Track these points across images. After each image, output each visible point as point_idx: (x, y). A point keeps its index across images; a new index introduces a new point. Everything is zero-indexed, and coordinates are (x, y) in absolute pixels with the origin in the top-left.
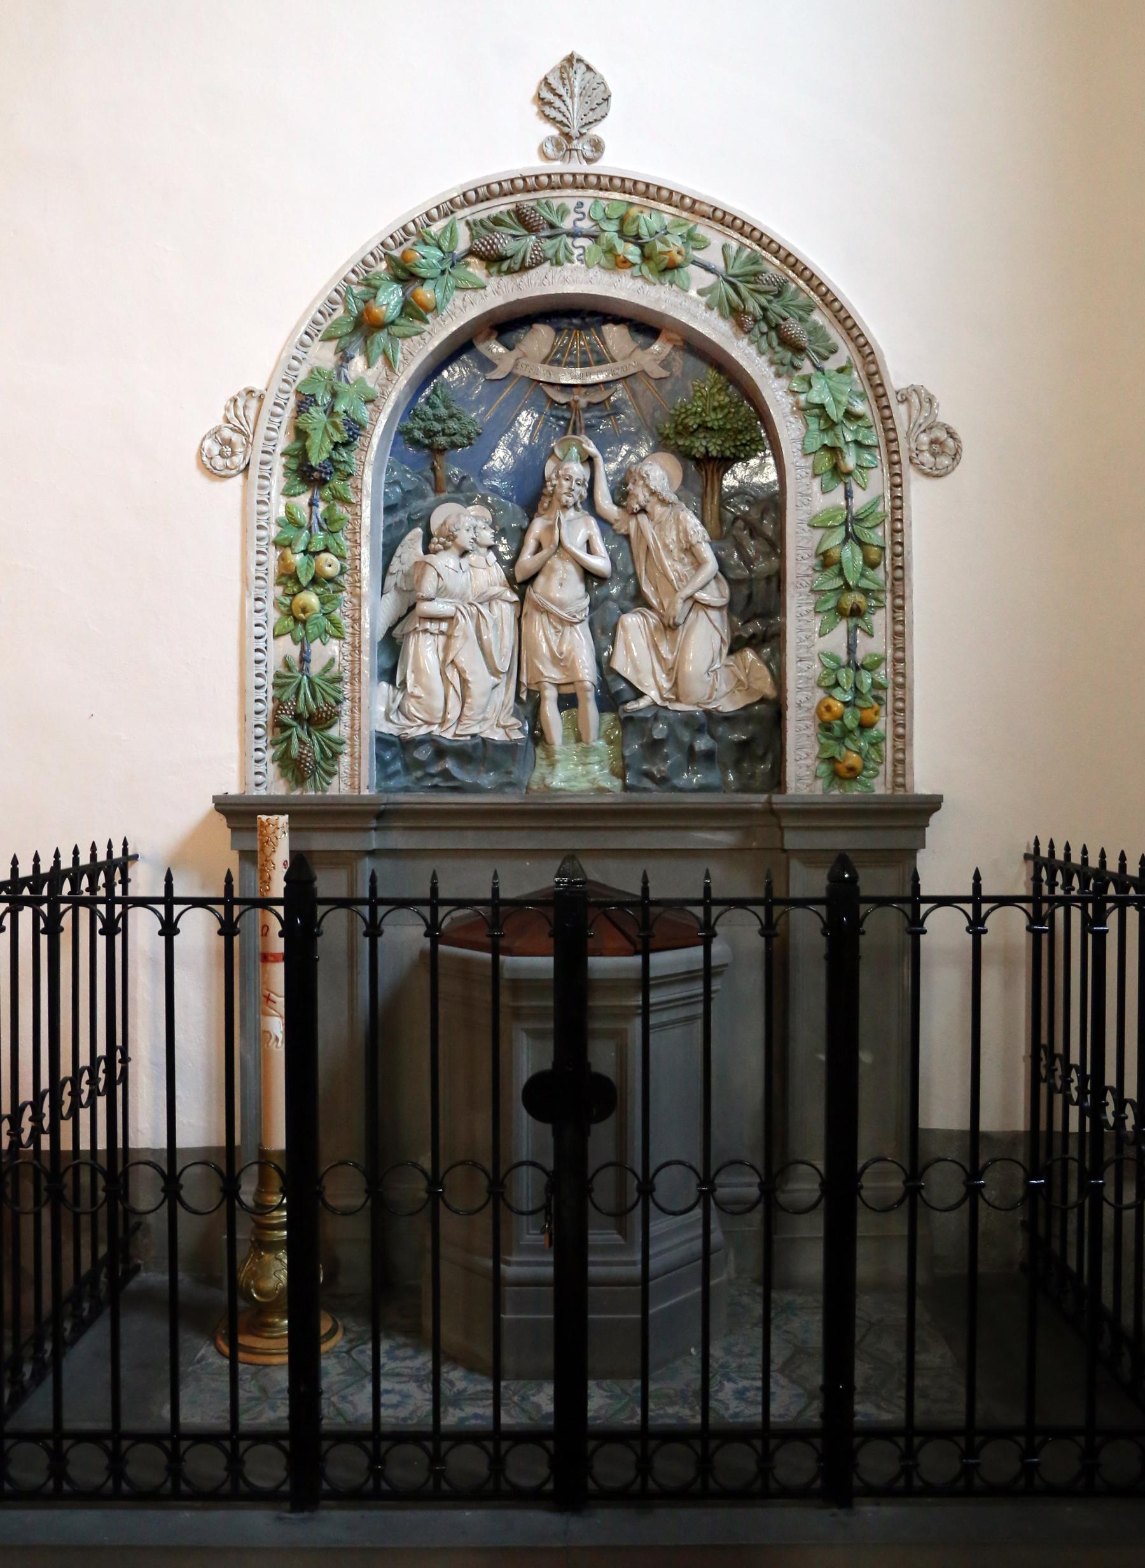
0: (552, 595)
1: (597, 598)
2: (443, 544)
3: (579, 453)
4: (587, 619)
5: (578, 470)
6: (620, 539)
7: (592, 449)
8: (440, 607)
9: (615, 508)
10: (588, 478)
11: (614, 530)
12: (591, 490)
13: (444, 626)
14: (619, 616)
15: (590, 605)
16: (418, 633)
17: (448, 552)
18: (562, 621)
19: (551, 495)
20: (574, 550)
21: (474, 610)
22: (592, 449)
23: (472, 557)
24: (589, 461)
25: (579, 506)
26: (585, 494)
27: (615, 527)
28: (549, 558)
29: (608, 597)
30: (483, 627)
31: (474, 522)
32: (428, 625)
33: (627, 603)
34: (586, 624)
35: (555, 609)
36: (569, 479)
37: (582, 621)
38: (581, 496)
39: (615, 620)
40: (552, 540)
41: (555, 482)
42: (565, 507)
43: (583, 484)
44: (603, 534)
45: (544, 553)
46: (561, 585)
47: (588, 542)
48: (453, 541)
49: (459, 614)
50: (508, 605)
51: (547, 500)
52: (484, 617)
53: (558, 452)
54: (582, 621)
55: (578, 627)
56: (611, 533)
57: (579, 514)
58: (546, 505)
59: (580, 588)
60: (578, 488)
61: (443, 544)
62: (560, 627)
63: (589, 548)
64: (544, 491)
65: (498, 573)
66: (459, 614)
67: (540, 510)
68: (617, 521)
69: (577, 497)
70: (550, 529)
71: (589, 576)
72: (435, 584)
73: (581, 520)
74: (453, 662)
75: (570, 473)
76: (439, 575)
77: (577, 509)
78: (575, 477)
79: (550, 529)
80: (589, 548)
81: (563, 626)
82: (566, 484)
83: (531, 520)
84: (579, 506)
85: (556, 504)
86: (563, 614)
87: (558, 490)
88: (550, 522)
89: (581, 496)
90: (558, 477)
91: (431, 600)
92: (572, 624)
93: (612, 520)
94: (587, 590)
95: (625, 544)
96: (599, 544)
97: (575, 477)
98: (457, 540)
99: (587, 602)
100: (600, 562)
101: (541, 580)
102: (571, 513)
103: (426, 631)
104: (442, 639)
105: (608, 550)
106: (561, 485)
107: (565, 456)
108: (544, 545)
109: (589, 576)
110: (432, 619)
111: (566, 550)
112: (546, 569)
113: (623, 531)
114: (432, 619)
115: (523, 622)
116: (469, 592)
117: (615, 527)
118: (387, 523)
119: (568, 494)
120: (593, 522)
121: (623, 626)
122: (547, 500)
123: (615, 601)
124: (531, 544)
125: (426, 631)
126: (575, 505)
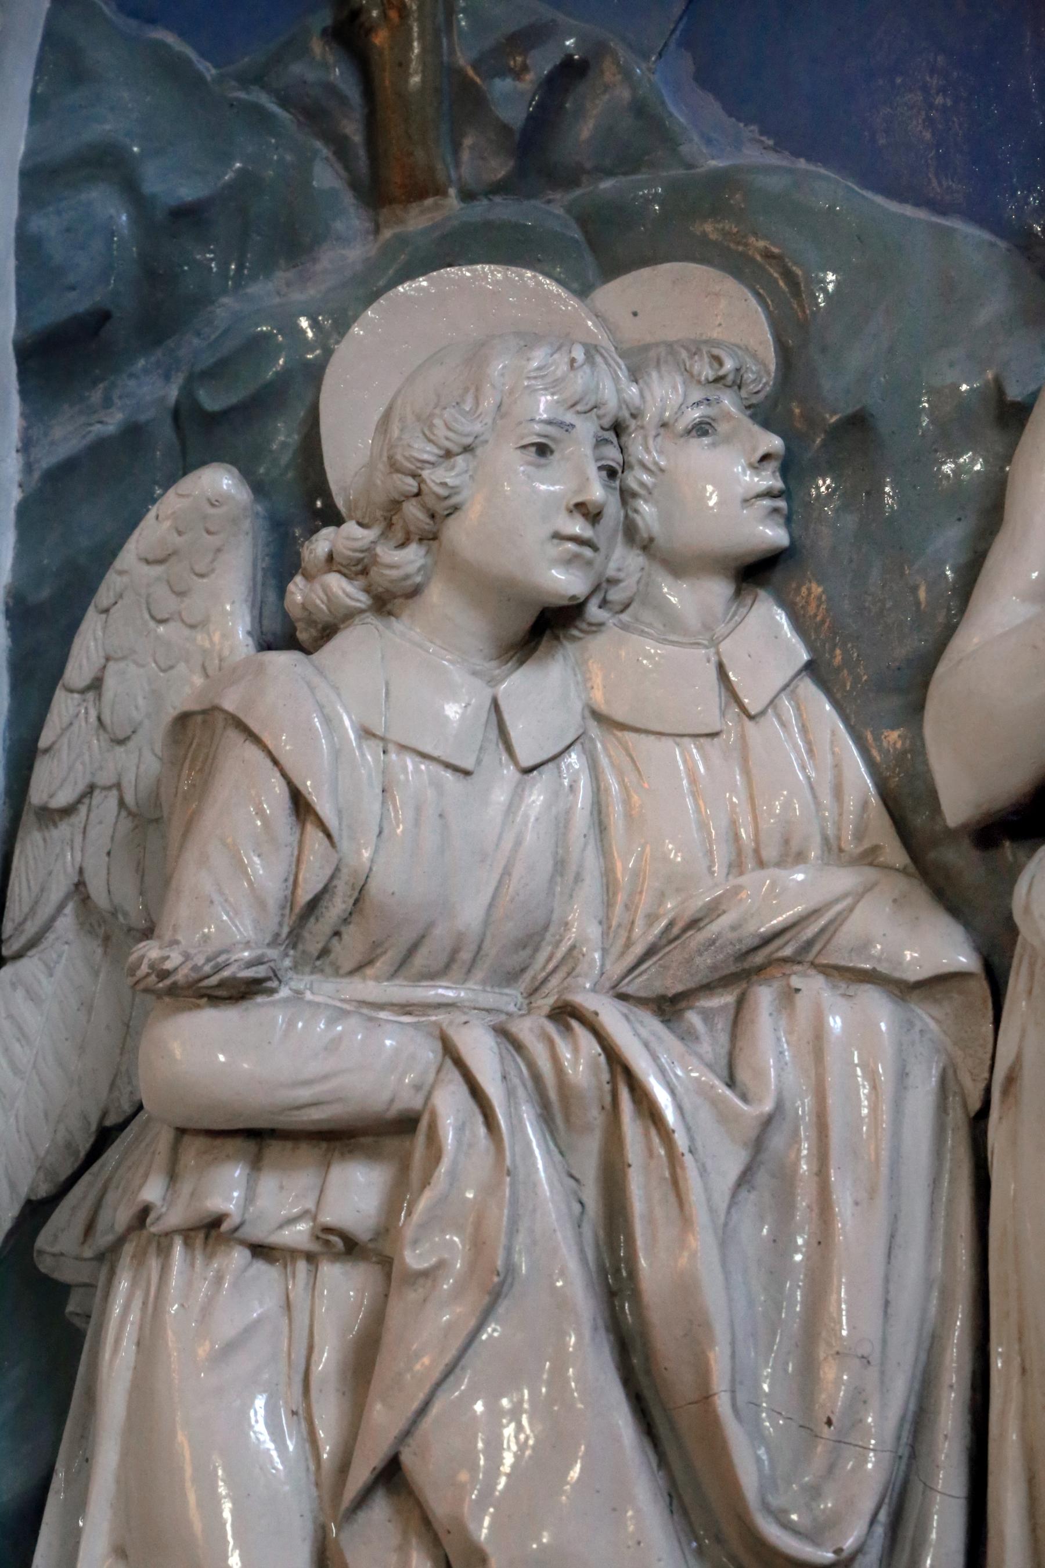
2: (359, 568)
8: (314, 1045)
13: (356, 1192)
16: (162, 1245)
17: (404, 631)
21: (579, 1060)
23: (609, 664)
30: (641, 1191)
31: (613, 389)
32: (225, 1187)
48: (430, 538)
49: (451, 1107)
50: (881, 1014)
52: (651, 1113)
61: (359, 568)
65: (814, 763)
66: (451, 1107)
72: (265, 872)
74: (391, 1475)
76: (300, 806)
91: (242, 991)
98: (460, 533)
103: (211, 1231)
104: (342, 1287)
110: (259, 1138)
114: (259, 1138)
116: (582, 923)
118: (47, 460)
125: (211, 1231)
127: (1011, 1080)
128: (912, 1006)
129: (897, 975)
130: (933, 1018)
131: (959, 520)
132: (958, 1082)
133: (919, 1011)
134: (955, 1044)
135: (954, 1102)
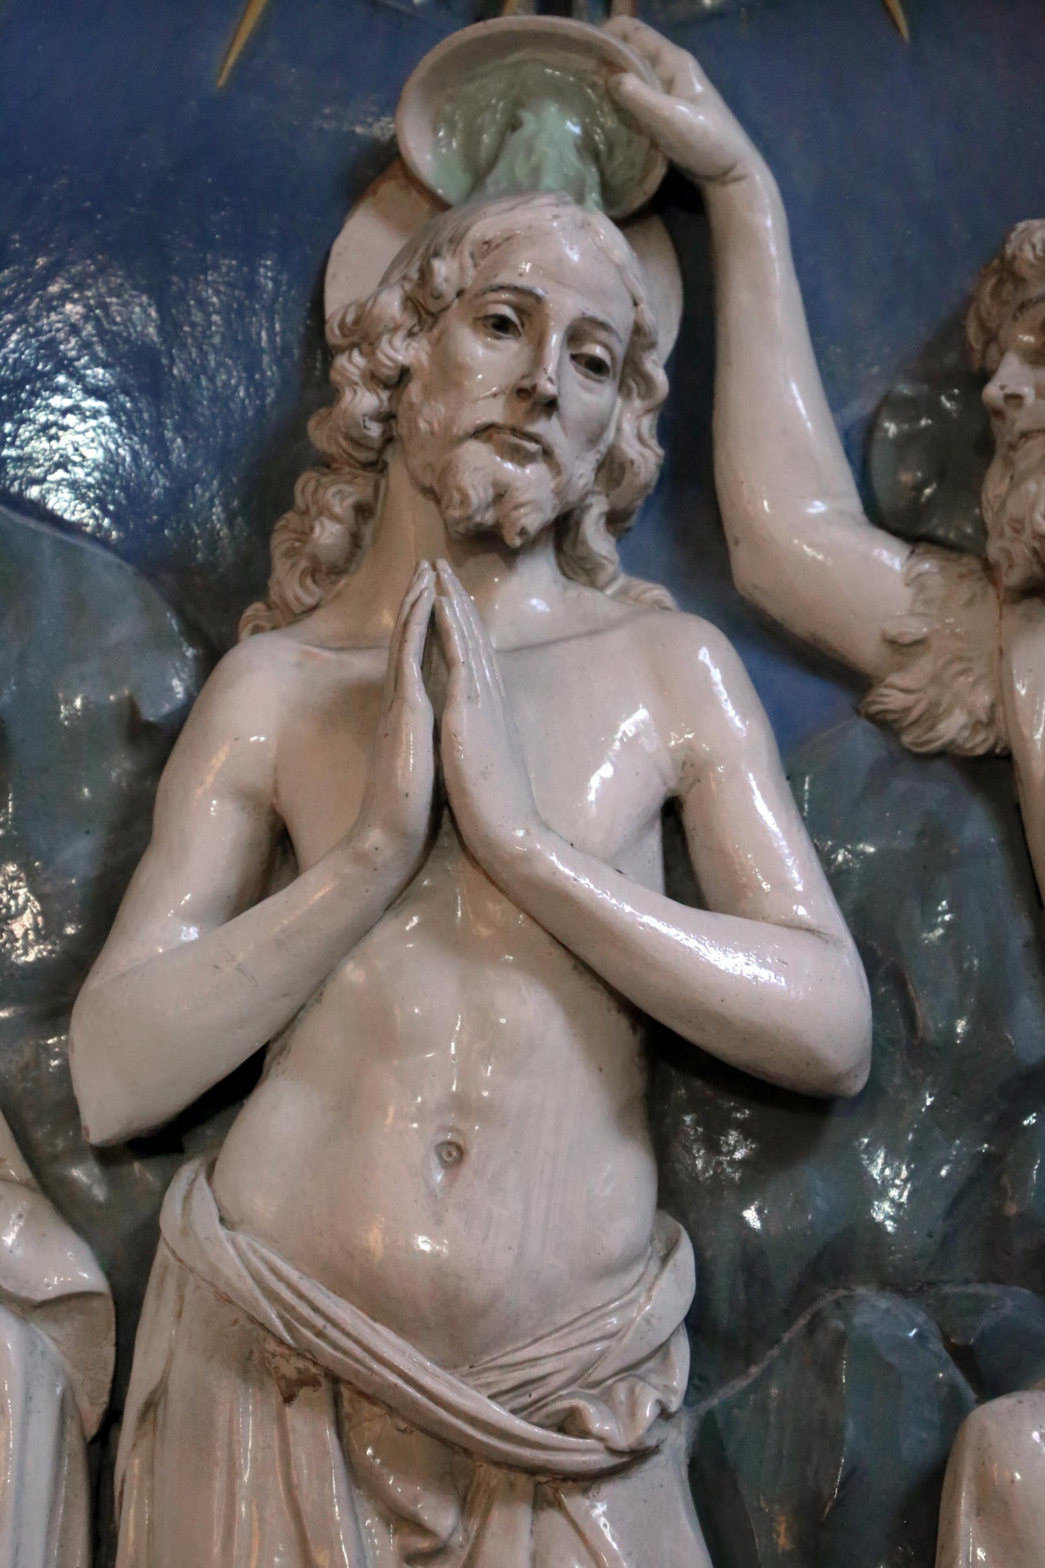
0: (374, 1239)
1: (752, 1255)
3: (587, 148)
4: (677, 1440)
5: (581, 257)
6: (937, 791)
7: (694, 111)
9: (890, 556)
10: (667, 338)
11: (886, 725)
12: (691, 419)
14: (953, 1414)
15: (698, 1322)
18: (462, 1464)
19: (377, 466)
20: (560, 865)
22: (694, 111)
24: (675, 209)
25: (598, 540)
26: (645, 457)
27: (890, 699)
28: (355, 937)
29: (844, 1255)
33: (1011, 1303)
34: (666, 1479)
35: (401, 1357)
36: (516, 318)
37: (635, 1458)
38: (612, 468)
39: (916, 1443)
40: (375, 795)
41: (400, 351)
42: (486, 544)
43: (628, 374)
44: (797, 752)
45: (313, 893)
46: (453, 1154)
47: (671, 812)
51: (339, 497)
53: (427, 149)
54: (635, 1458)
55: (598, 1511)
56: (861, 743)
57: (599, 603)
58: (328, 534)
59: (620, 1179)
60: (584, 398)
62: (442, 1517)
63: (682, 853)
64: (320, 435)
67: (288, 583)
68: (902, 649)
69: (582, 470)
70: (366, 710)
71: (680, 1074)
73: (617, 641)
75: (524, 270)
77: (576, 566)
78: (564, 307)
79: (366, 710)
80: (683, 857)
81: (469, 1502)
82: (489, 363)
83: (212, 653)
84: (598, 540)
85: (410, 517)
86: (472, 1399)
87: (429, 415)
88: (366, 665)
89: (612, 468)
90: (425, 311)
92: (549, 1487)
93: (865, 650)
94: (673, 1195)
95: (977, 826)
96: (761, 819)
97: (564, 307)
99: (673, 1291)
100: (777, 967)
101: (279, 1117)
102: (535, 591)
105: (837, 880)
106: (449, 372)
107: (479, 173)
108: (307, 837)
109: (680, 1074)
111: (500, 877)
112: (324, 1034)
113: (952, 727)
115: (129, 1462)
117: (890, 699)
119: (512, 440)
120: (712, 661)
121: (997, 1507)
122: (339, 497)
123: (903, 1285)
124: (204, 830)
126: (563, 530)
127: (150, 1406)
128: (33, 1326)
129: (24, 1294)
130: (53, 1339)
131: (88, 832)
132: (76, 1406)
133: (39, 1332)
134: (75, 1366)
135: (72, 1427)
